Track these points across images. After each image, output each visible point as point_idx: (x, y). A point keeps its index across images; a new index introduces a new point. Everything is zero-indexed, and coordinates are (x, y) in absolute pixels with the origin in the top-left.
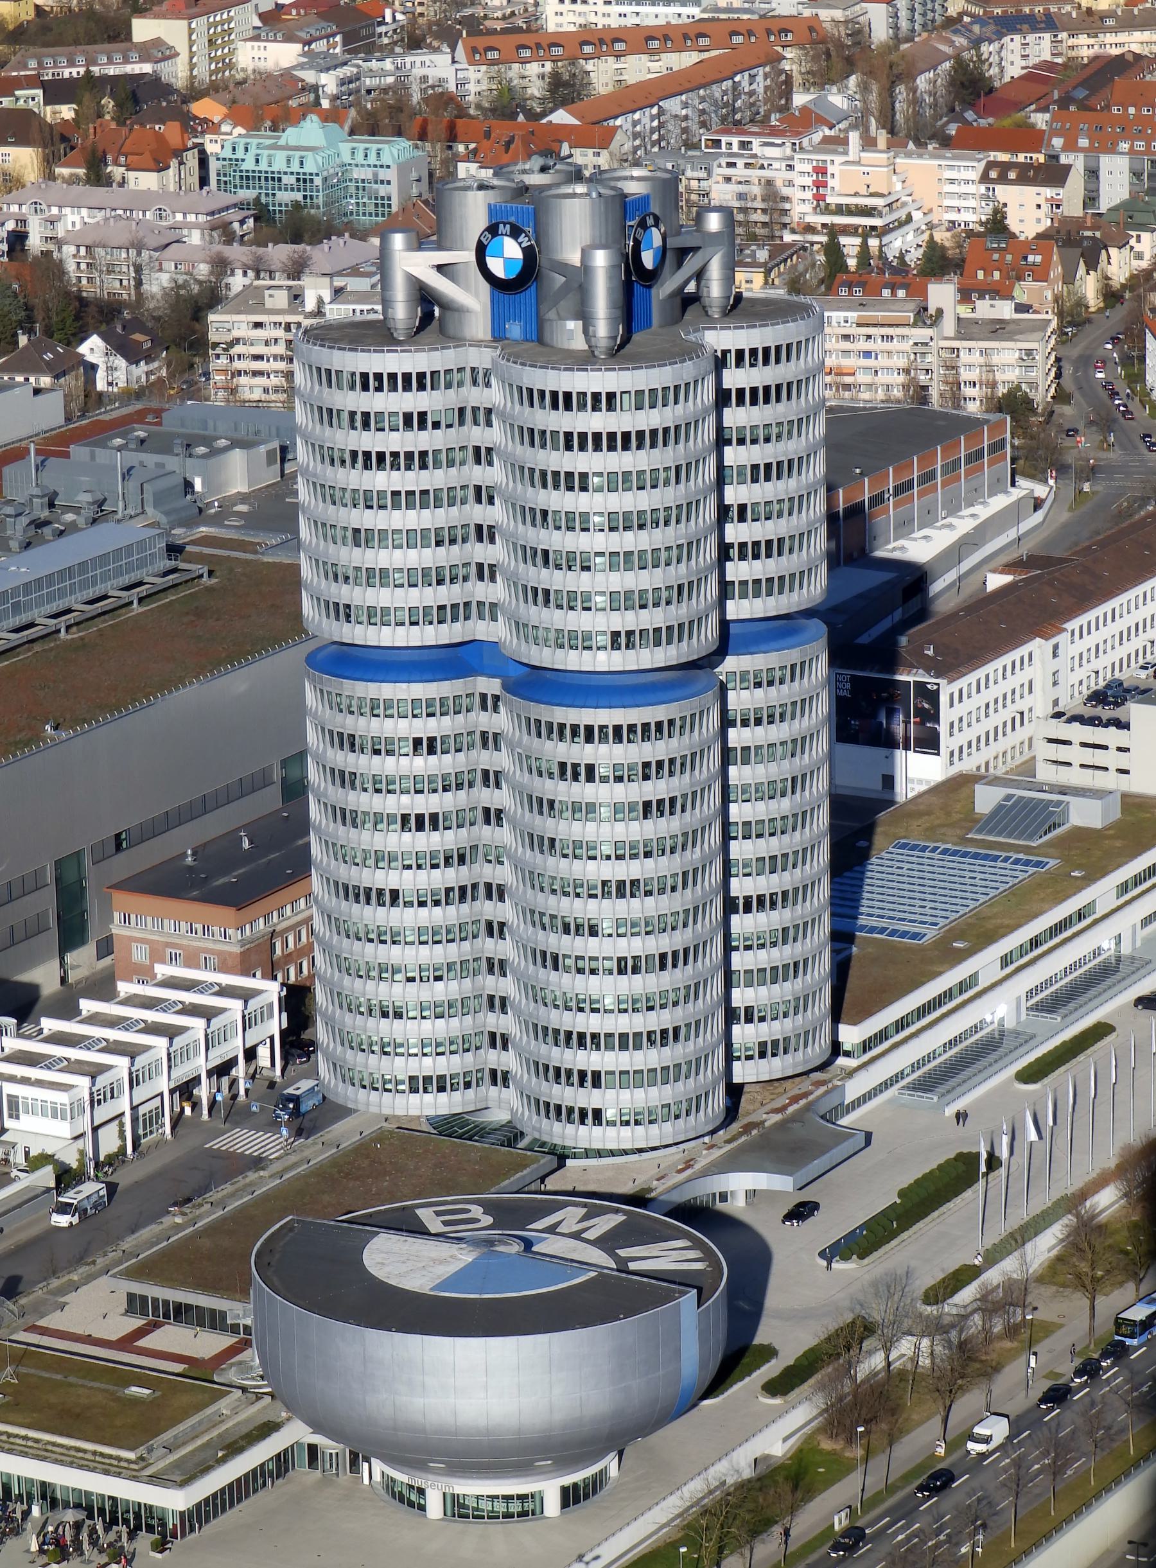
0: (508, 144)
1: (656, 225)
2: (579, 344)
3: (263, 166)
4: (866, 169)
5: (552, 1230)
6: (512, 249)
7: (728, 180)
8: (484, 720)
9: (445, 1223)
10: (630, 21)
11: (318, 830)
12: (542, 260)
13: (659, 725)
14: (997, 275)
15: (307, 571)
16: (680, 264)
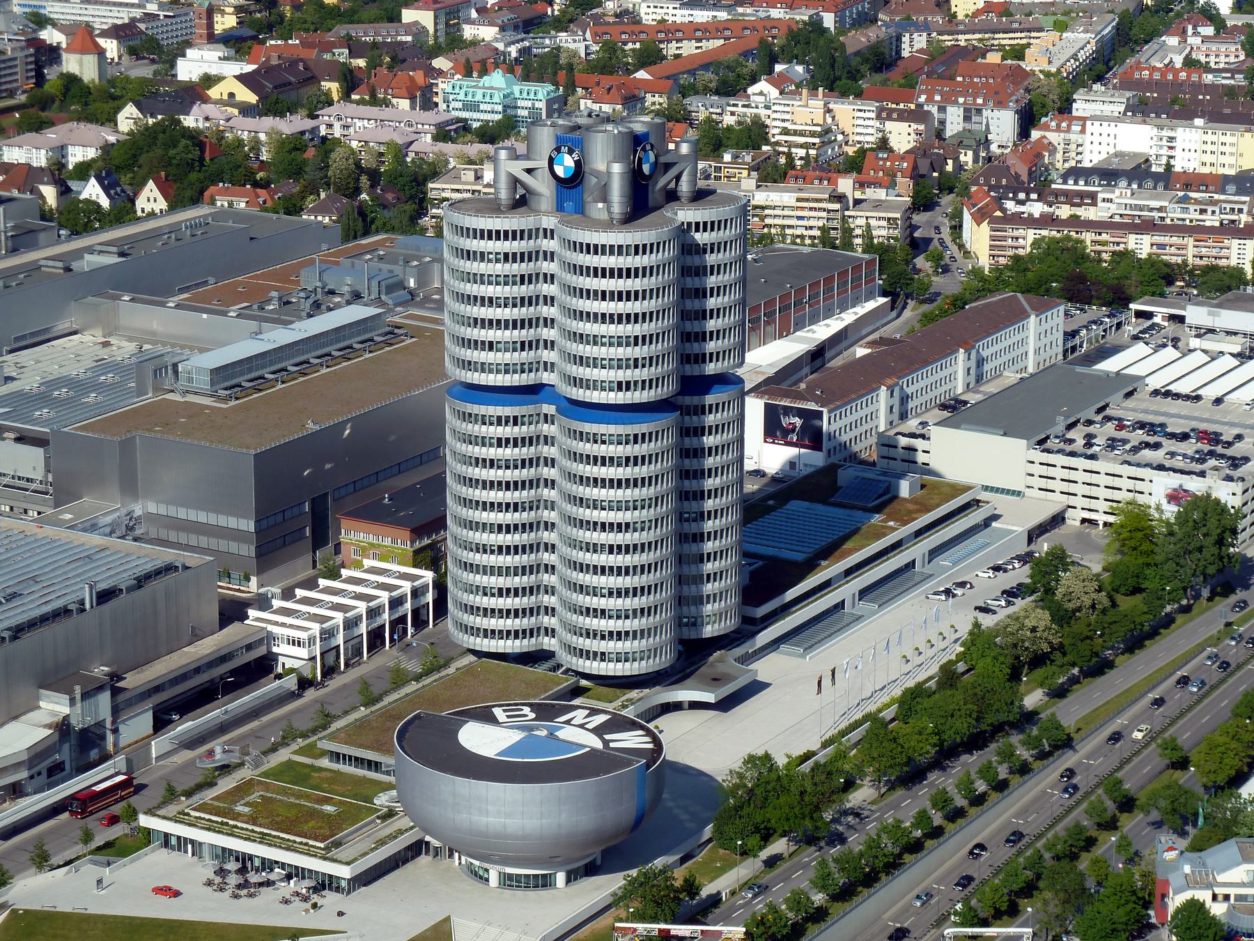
0: (609, 89)
1: (652, 150)
2: (604, 216)
3: (469, 98)
4: (812, 110)
5: (568, 722)
6: (569, 161)
7: (733, 114)
8: (546, 429)
9: (508, 717)
10: (687, 20)
11: (451, 488)
12: (586, 169)
13: (643, 435)
14: (881, 174)
15: (447, 342)
16: (666, 172)
